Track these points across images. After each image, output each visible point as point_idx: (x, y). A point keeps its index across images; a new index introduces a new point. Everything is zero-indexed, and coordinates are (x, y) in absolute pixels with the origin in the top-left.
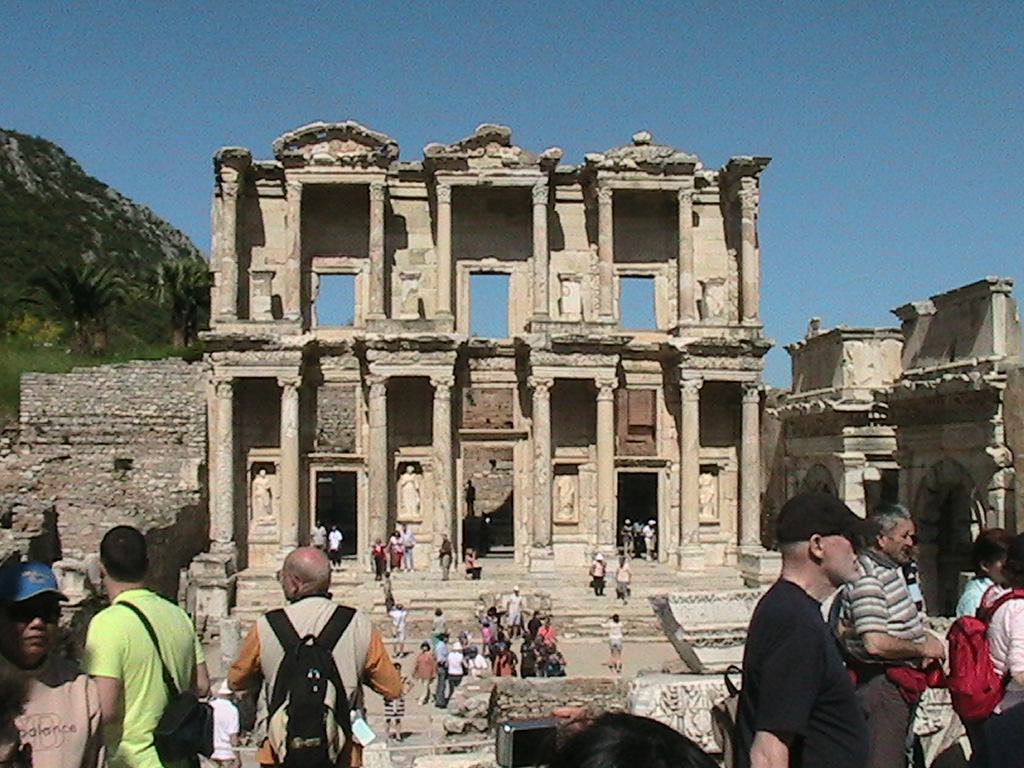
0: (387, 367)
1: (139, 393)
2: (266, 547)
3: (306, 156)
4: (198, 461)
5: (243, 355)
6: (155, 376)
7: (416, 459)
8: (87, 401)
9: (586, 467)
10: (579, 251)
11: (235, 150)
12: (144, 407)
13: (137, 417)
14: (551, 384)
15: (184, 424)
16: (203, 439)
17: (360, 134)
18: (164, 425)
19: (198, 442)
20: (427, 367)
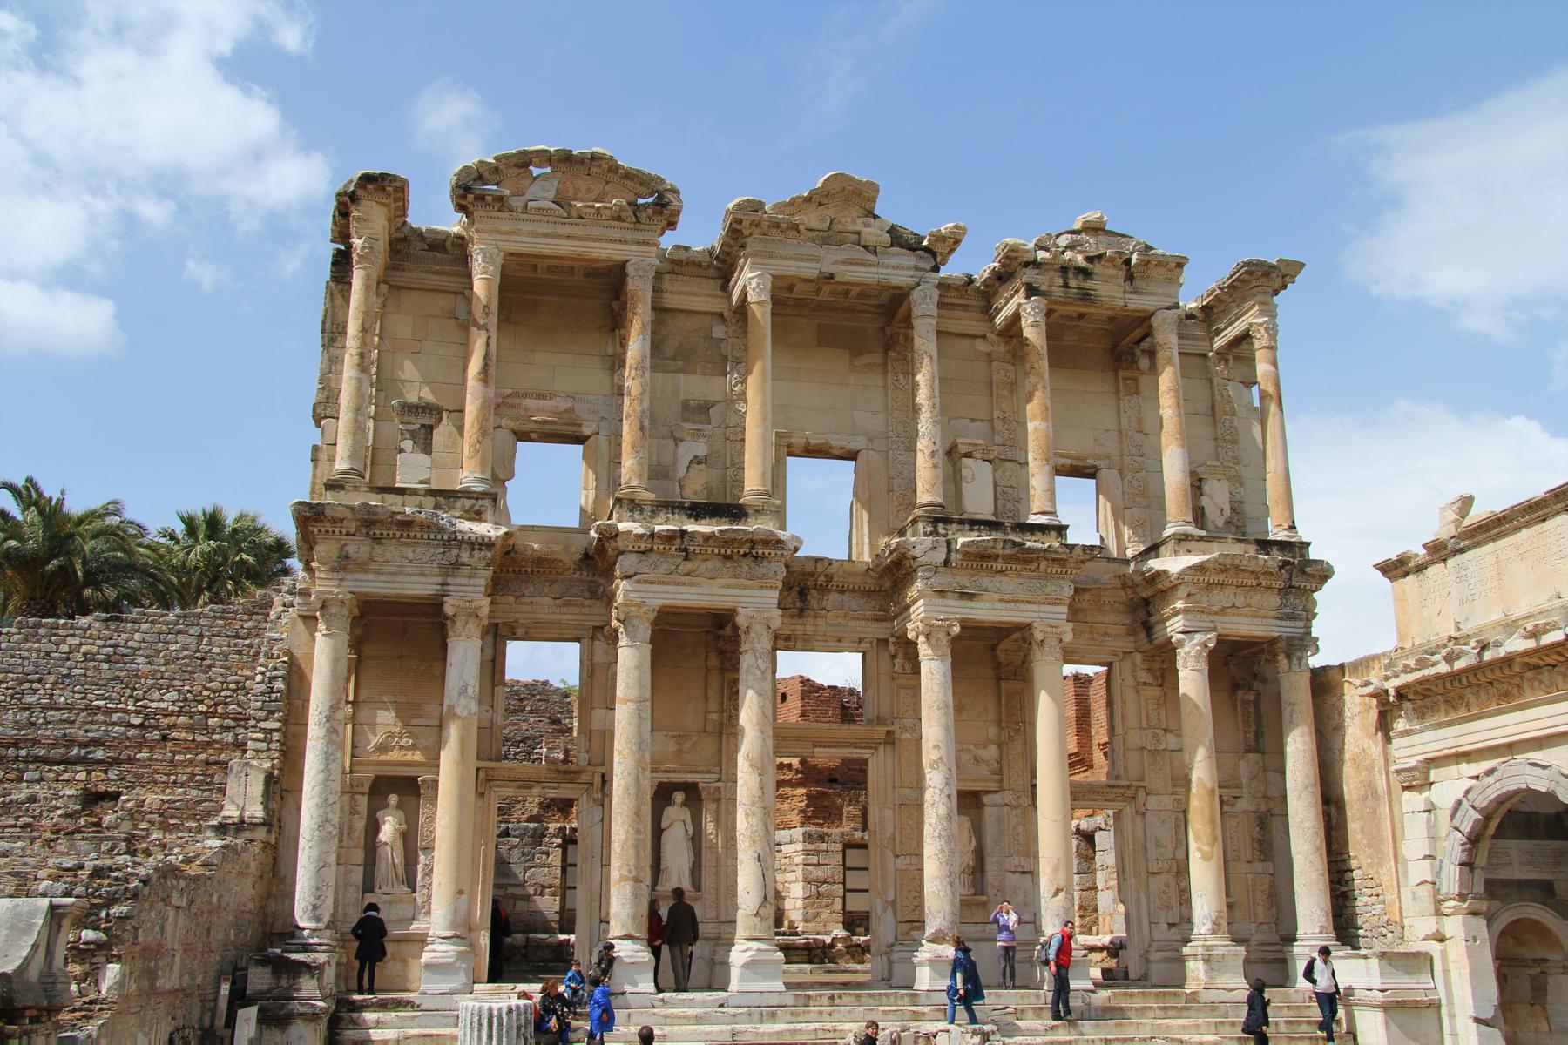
0: (656, 588)
1: (145, 668)
3: (517, 203)
4: (267, 765)
5: (378, 550)
6: (180, 638)
7: (689, 778)
8: (39, 681)
9: (996, 798)
10: (973, 420)
11: (383, 176)
12: (156, 695)
13: (138, 713)
14: (957, 630)
15: (228, 729)
16: (277, 725)
17: (614, 168)
18: (190, 728)
19: (272, 730)
20: (731, 591)
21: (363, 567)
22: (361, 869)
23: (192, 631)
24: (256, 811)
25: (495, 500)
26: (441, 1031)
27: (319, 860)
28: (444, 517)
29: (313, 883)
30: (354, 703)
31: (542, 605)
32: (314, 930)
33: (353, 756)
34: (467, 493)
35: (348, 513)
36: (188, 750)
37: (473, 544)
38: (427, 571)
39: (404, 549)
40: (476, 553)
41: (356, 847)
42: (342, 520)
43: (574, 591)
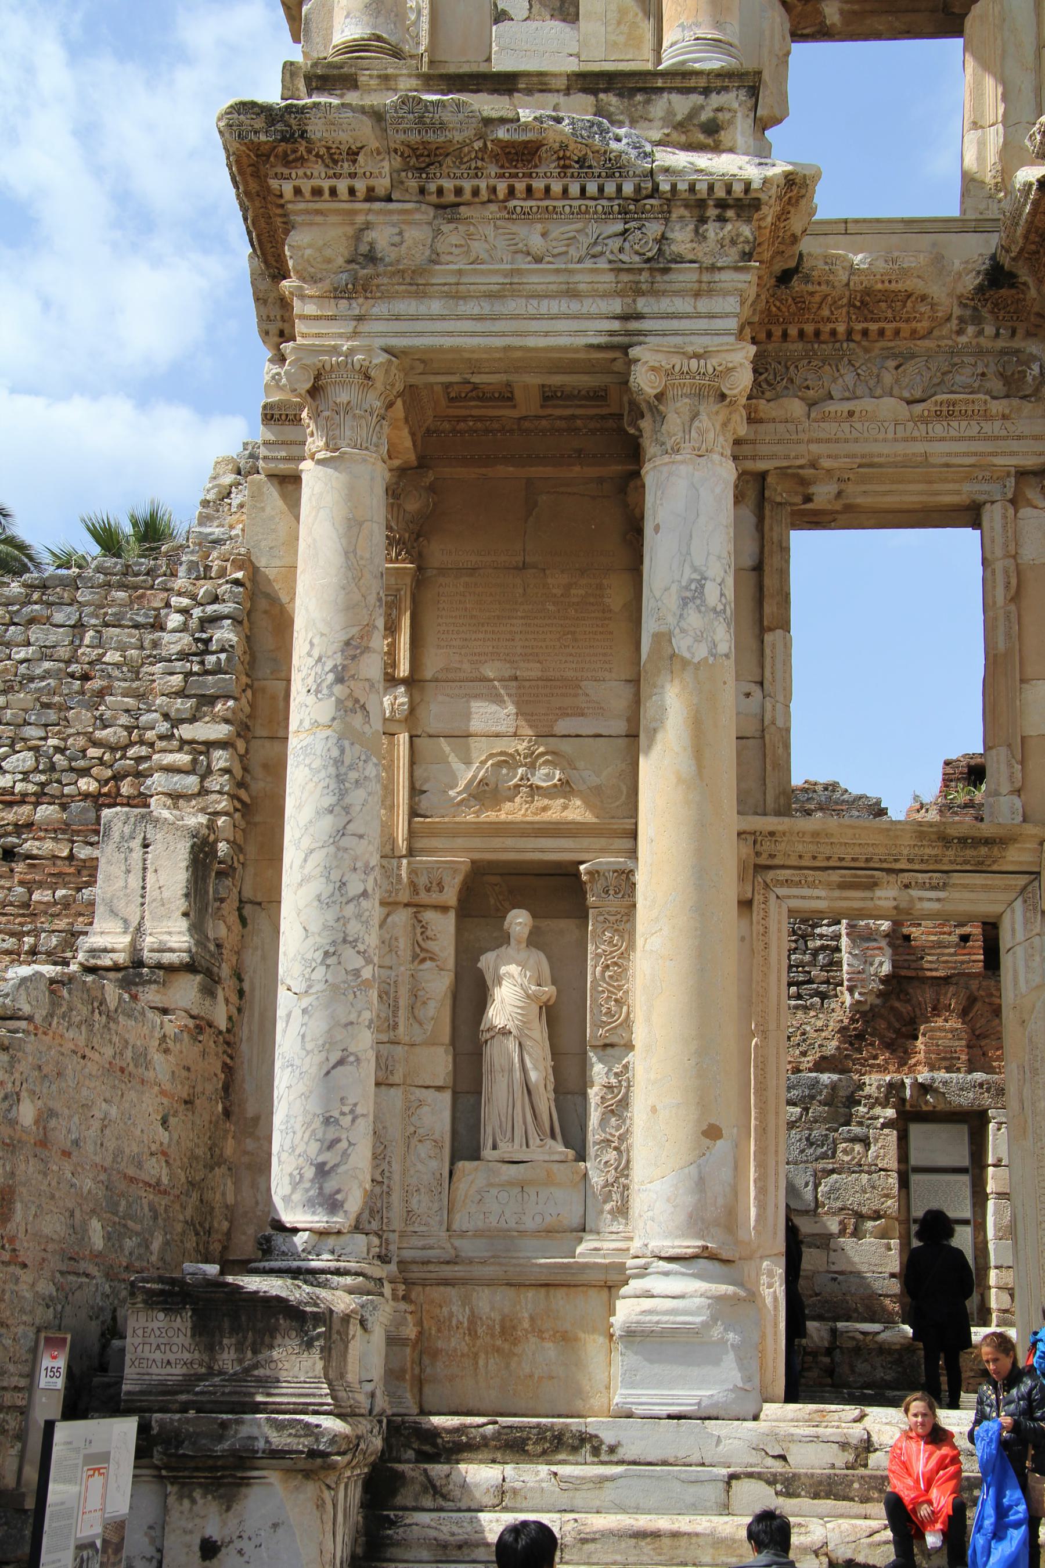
2: (529, 1302)
4: (196, 820)
5: (452, 236)
6: (35, 633)
18: (63, 830)
19: (210, 745)
21: (415, 281)
22: (447, 1097)
23: (59, 617)
24: (171, 935)
25: (754, 92)
26: (683, 1523)
27: (329, 1043)
28: (623, 140)
29: (314, 1106)
30: (411, 682)
31: (873, 422)
32: (322, 1234)
33: (413, 813)
34: (682, 79)
35: (365, 132)
36: (59, 879)
37: (701, 204)
38: (582, 281)
39: (520, 230)
40: (711, 229)
42: (353, 154)
43: (962, 378)
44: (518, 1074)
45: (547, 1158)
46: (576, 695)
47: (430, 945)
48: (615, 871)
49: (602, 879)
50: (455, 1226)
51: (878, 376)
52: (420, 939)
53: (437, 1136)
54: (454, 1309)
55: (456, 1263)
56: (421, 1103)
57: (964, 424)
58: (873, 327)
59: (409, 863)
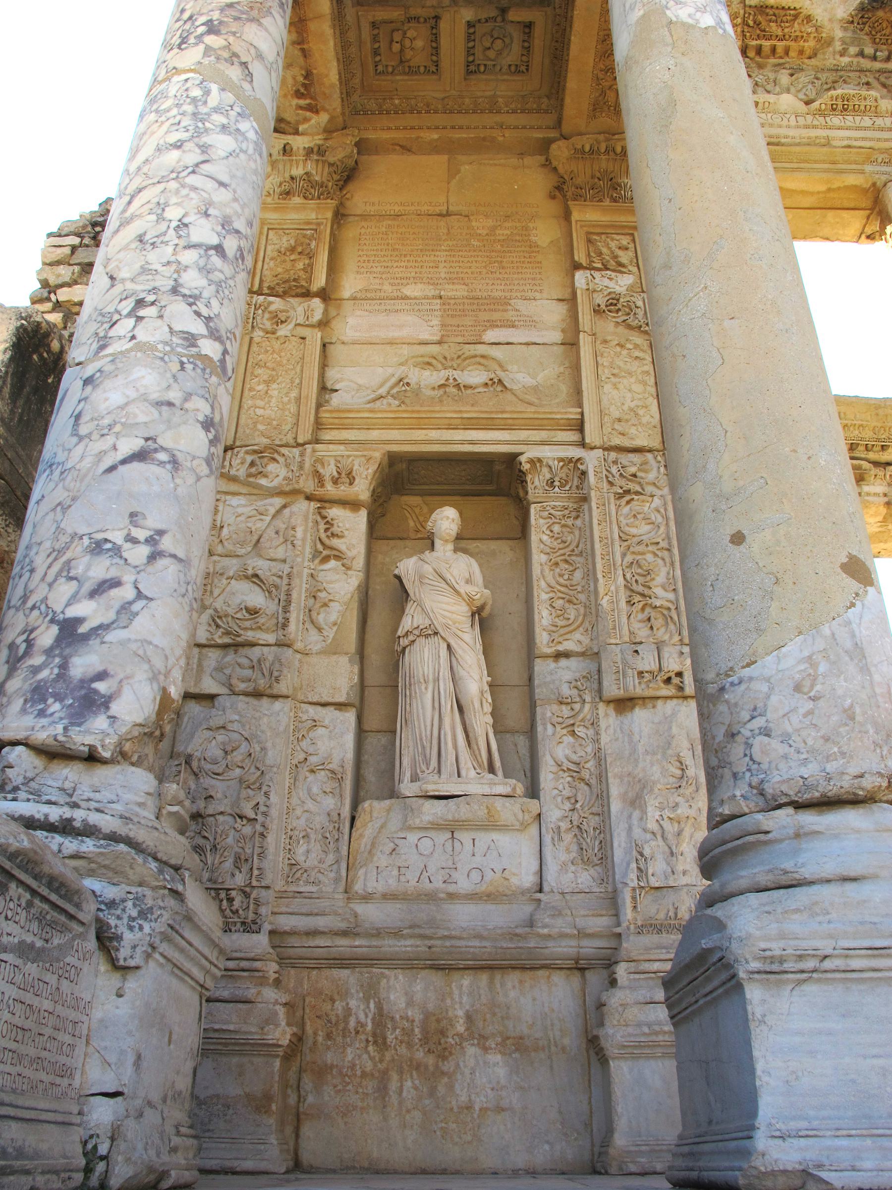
2: (463, 994)
22: (350, 716)
41: (333, 650)
44: (446, 686)
45: (487, 790)
46: (506, 311)
47: (335, 542)
48: (561, 460)
49: (545, 470)
50: (358, 887)
51: (775, 81)
52: (323, 536)
53: (334, 766)
54: (353, 1003)
55: (357, 935)
56: (315, 724)
57: (858, 119)
58: (766, 44)
59: (314, 451)
